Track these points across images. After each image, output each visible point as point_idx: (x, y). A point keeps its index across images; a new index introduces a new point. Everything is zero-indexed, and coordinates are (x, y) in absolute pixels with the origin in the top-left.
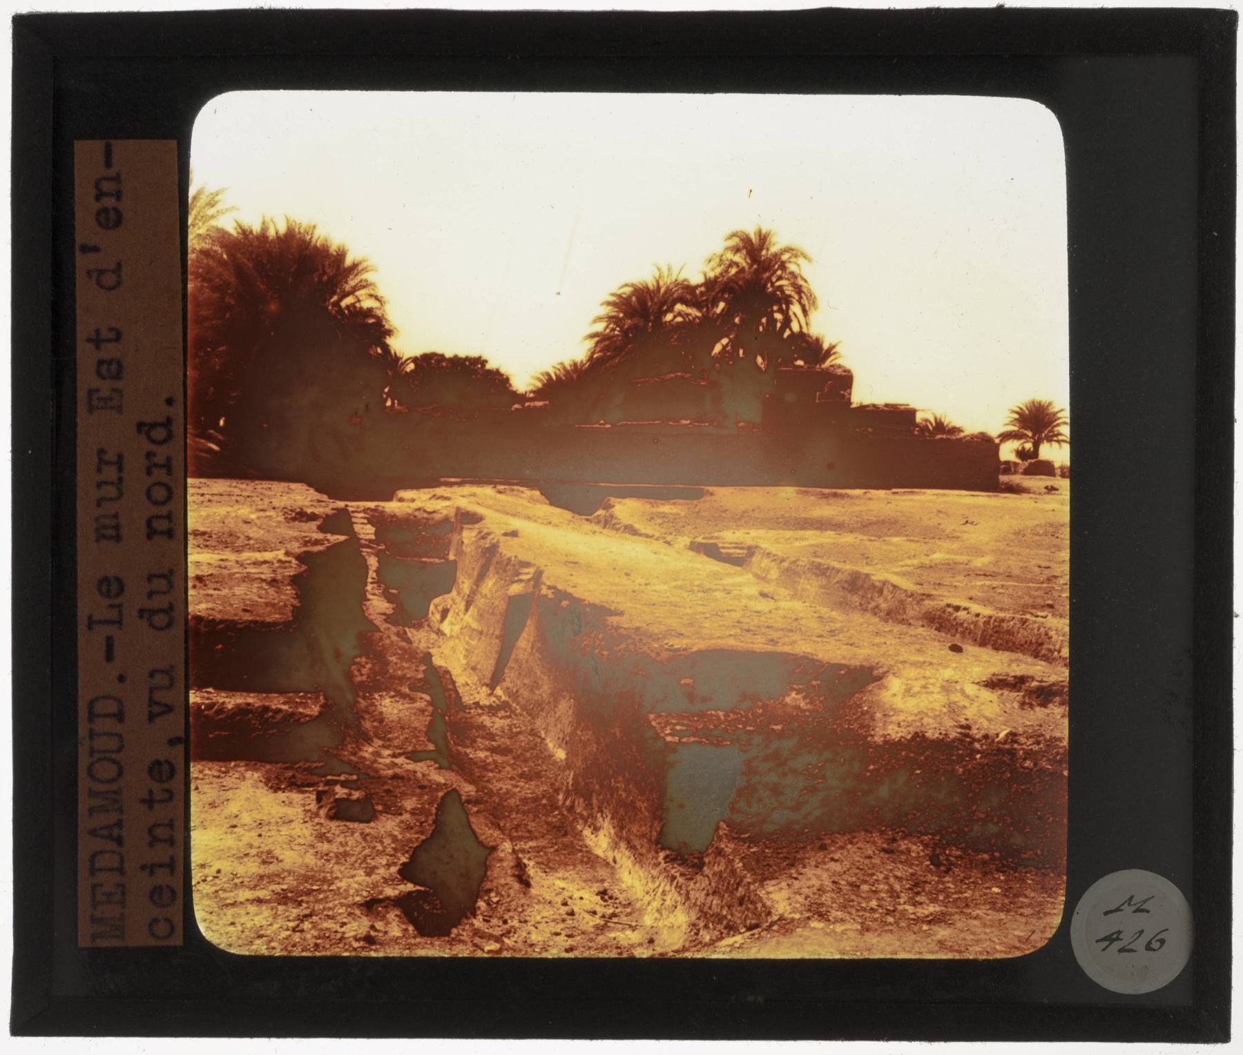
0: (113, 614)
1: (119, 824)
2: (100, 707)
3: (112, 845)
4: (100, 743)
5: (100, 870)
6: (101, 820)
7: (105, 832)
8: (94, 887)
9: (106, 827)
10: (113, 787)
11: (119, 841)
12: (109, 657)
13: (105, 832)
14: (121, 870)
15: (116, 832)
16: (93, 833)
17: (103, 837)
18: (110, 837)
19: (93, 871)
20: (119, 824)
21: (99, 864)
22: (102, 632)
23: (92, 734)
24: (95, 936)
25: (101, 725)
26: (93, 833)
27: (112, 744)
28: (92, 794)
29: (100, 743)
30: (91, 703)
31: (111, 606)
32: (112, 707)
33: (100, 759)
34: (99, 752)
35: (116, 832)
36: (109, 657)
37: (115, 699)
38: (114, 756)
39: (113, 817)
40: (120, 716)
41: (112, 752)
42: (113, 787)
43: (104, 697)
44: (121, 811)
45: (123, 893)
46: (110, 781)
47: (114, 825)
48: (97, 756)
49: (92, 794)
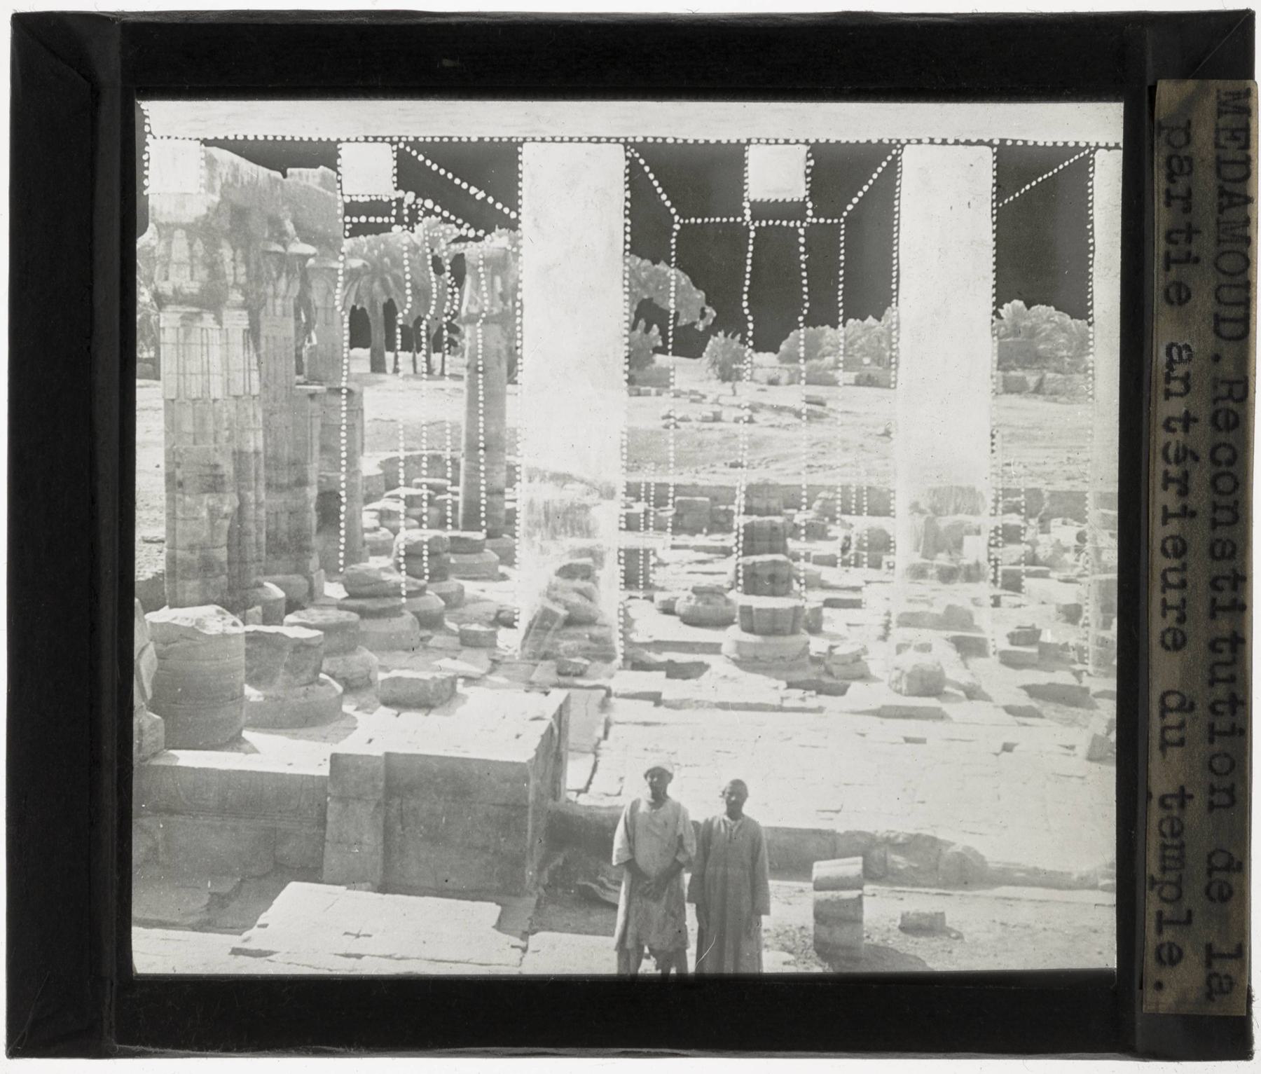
3: (1228, 187)
7: (1236, 200)
9: (1235, 205)
10: (1227, 247)
11: (1222, 192)
13: (1236, 200)
15: (1225, 201)
17: (1239, 196)
18: (1231, 195)
20: (1221, 211)
27: (1226, 294)
32: (1227, 329)
38: (1224, 280)
40: (1218, 319)
42: (1227, 247)
44: (1218, 223)
45: (1217, 138)
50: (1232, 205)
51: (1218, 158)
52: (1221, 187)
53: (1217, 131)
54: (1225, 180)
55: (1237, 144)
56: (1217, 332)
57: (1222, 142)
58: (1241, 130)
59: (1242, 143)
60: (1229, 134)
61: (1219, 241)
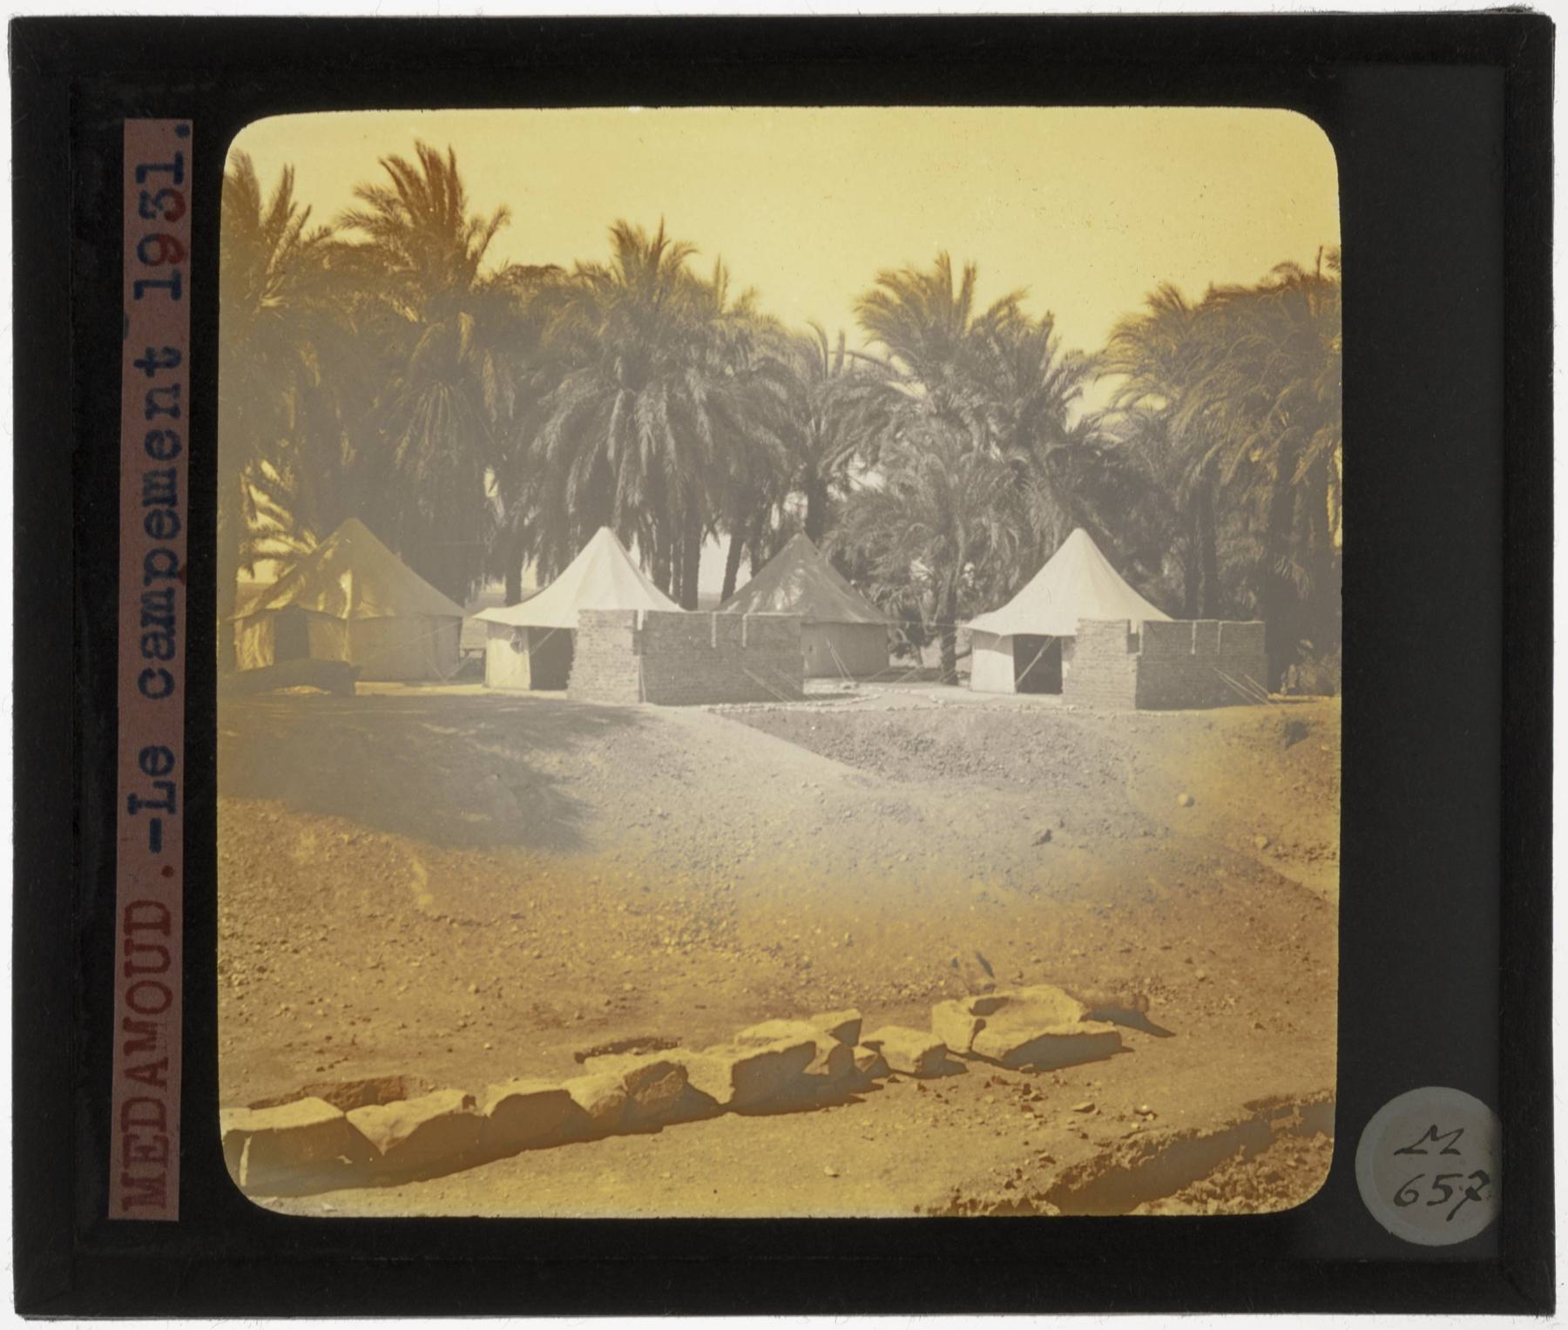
0: (161, 795)
1: (164, 1064)
4: (138, 959)
6: (141, 1058)
8: (128, 1140)
14: (161, 1124)
16: (131, 1073)
17: (143, 1079)
18: (152, 1080)
21: (138, 1112)
22: (146, 814)
23: (129, 946)
24: (127, 1203)
25: (141, 937)
26: (131, 1073)
27: (155, 959)
29: (138, 959)
31: (158, 785)
32: (153, 915)
33: (143, 983)
37: (160, 906)
43: (149, 904)
50: (153, 1068)
53: (164, 1160)
57: (158, 1145)
59: (133, 1146)
60: (152, 1154)
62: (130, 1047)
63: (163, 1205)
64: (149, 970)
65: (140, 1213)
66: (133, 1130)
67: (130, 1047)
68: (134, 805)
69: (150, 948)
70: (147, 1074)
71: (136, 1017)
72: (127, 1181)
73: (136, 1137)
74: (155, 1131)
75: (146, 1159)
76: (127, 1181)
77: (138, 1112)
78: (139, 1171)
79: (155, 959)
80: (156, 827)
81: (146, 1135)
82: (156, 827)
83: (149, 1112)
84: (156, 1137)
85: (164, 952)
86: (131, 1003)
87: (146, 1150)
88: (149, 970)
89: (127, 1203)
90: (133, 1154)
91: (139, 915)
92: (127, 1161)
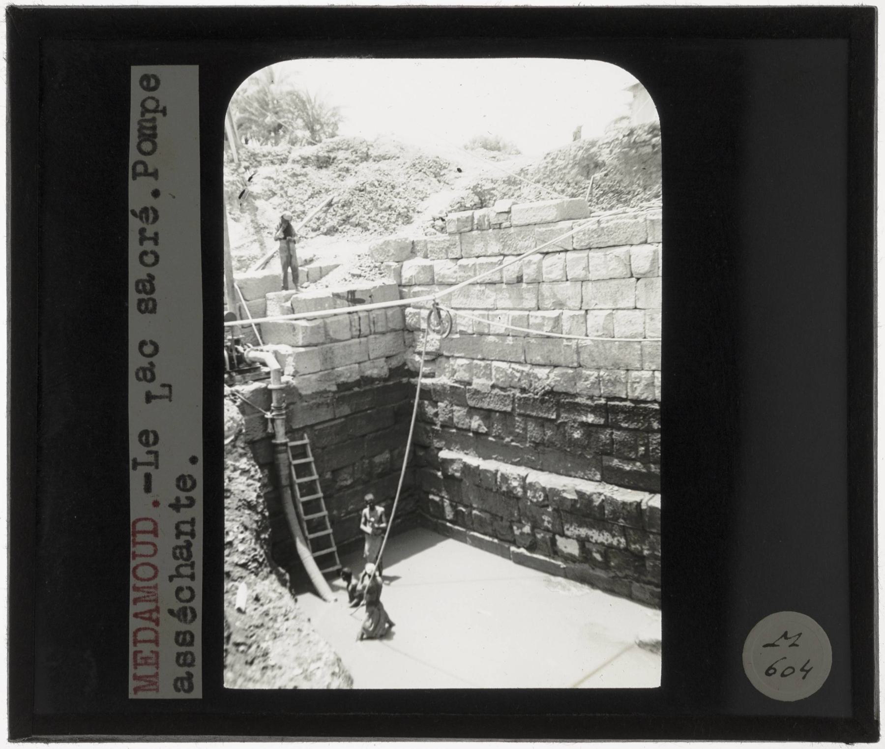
0: (151, 458)
2: (140, 526)
3: (152, 625)
5: (140, 642)
8: (136, 653)
9: (145, 613)
10: (151, 583)
12: (148, 489)
14: (156, 642)
15: (154, 615)
16: (136, 615)
17: (143, 618)
18: (150, 619)
19: (135, 644)
21: (141, 636)
22: (142, 470)
24: (136, 690)
25: (140, 538)
26: (136, 615)
28: (136, 589)
30: (135, 523)
32: (149, 526)
33: (143, 564)
34: (142, 556)
35: (154, 615)
36: (148, 489)
37: (153, 521)
39: (152, 606)
40: (155, 532)
41: (151, 556)
42: (151, 583)
43: (146, 519)
44: (156, 601)
46: (149, 580)
47: (150, 611)
48: (139, 560)
49: (136, 589)
51: (157, 644)
52: (157, 624)
53: (157, 665)
54: (152, 629)
55: (144, 655)
56: (155, 524)
57: (154, 656)
58: (140, 665)
59: (139, 656)
60: (150, 661)
61: (156, 587)
62: (136, 601)
63: (157, 690)
64: (147, 556)
65: (141, 695)
66: (140, 647)
67: (136, 601)
68: (136, 464)
69: (147, 543)
70: (147, 615)
71: (140, 584)
72: (136, 678)
73: (141, 652)
74: (153, 647)
75: (146, 664)
76: (136, 678)
77: (141, 636)
78: (143, 671)
79: (149, 550)
80: (148, 477)
81: (146, 649)
82: (148, 477)
83: (150, 635)
84: (152, 652)
85: (154, 545)
86: (136, 576)
87: (146, 658)
88: (147, 556)
89: (136, 690)
90: (139, 661)
91: (140, 526)
92: (136, 665)
